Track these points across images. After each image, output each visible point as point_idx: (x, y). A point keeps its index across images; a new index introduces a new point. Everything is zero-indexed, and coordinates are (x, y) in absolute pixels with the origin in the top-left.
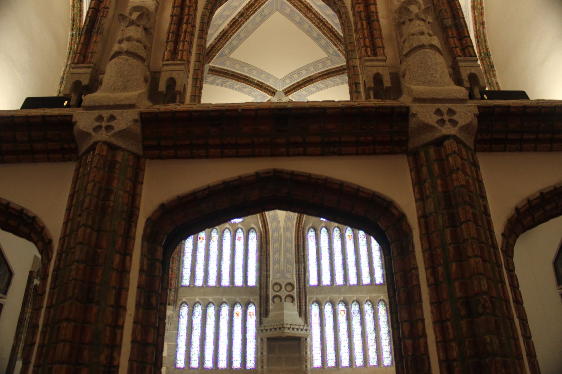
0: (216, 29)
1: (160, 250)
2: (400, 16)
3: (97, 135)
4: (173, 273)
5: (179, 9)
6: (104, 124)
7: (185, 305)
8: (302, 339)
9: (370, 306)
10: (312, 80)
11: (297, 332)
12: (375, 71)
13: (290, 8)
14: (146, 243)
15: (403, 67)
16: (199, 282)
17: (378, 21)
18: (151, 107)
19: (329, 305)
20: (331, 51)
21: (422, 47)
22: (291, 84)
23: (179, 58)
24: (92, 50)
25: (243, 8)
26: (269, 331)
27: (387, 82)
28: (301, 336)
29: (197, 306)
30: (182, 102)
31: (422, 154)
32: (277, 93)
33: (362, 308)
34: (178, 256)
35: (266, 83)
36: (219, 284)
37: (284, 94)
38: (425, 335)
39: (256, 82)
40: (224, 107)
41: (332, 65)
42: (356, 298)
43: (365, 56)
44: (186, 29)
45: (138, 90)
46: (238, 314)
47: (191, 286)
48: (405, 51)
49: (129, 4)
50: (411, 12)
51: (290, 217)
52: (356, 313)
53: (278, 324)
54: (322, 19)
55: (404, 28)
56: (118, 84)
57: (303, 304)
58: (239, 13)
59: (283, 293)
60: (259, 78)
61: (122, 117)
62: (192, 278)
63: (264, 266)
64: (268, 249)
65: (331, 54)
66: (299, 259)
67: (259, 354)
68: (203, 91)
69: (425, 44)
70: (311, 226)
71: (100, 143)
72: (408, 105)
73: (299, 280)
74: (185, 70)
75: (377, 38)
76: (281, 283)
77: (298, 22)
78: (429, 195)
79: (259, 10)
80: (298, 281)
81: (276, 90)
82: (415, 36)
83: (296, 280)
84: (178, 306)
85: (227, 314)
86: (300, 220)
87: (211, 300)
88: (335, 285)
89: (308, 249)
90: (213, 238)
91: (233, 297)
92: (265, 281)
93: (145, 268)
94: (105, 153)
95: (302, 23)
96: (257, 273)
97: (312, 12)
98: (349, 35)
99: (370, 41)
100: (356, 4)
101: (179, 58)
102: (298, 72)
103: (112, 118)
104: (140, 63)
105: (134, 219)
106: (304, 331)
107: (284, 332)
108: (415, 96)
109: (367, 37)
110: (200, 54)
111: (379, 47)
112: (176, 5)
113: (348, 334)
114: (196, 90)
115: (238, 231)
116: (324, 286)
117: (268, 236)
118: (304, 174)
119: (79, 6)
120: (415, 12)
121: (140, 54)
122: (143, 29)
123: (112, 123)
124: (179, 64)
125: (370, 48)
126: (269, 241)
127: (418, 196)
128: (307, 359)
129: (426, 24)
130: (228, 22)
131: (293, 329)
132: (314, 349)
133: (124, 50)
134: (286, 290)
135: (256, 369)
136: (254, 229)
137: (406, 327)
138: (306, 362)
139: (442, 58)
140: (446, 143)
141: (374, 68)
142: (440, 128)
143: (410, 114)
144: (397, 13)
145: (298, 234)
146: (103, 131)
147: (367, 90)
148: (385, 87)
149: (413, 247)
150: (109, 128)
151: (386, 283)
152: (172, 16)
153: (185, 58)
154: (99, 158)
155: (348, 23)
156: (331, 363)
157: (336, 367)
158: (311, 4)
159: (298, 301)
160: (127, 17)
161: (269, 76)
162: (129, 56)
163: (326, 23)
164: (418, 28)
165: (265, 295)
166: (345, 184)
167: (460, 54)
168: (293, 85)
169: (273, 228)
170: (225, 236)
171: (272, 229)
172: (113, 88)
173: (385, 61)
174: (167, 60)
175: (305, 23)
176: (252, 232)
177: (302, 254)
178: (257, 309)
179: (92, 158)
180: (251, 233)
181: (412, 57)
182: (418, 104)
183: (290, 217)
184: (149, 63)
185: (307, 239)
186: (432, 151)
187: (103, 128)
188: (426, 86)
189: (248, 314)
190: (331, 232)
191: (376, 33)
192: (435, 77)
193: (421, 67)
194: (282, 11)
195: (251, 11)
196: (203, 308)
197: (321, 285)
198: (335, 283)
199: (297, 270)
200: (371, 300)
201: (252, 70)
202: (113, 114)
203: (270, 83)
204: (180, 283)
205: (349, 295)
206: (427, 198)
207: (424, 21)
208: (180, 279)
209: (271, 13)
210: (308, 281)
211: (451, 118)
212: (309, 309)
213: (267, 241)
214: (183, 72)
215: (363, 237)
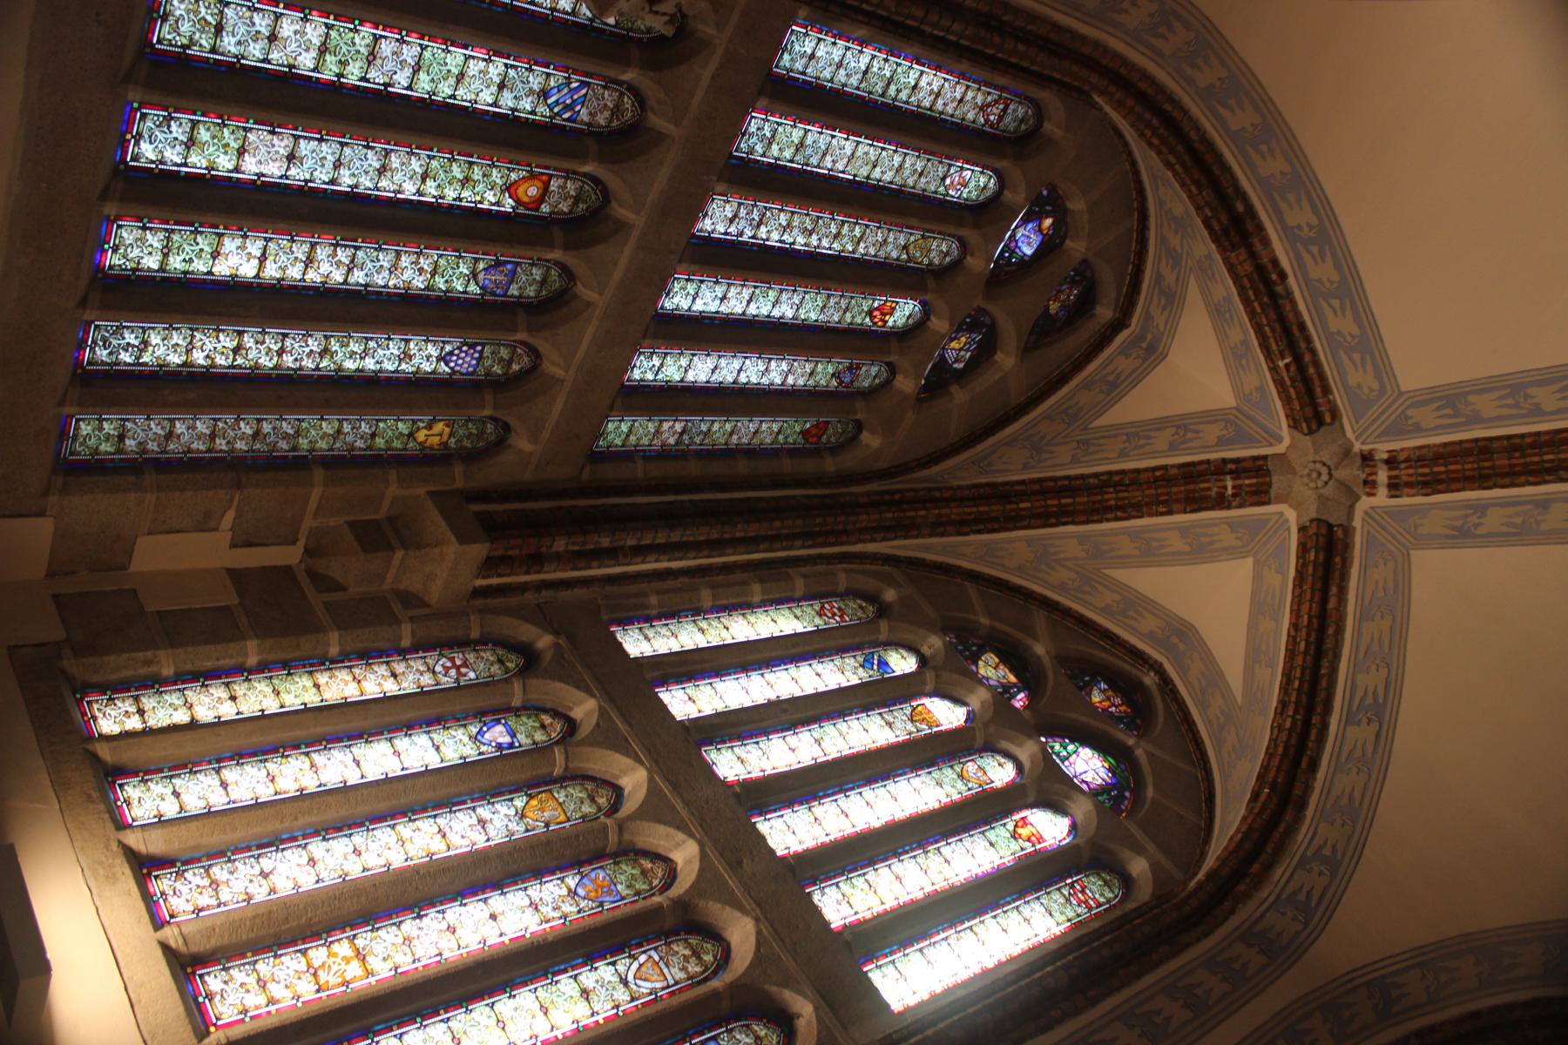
9: (497, 369)
19: (617, 110)
42: (589, 305)
70: (1047, 125)
205: (623, 262)
210: (814, 23)
215: (847, 380)
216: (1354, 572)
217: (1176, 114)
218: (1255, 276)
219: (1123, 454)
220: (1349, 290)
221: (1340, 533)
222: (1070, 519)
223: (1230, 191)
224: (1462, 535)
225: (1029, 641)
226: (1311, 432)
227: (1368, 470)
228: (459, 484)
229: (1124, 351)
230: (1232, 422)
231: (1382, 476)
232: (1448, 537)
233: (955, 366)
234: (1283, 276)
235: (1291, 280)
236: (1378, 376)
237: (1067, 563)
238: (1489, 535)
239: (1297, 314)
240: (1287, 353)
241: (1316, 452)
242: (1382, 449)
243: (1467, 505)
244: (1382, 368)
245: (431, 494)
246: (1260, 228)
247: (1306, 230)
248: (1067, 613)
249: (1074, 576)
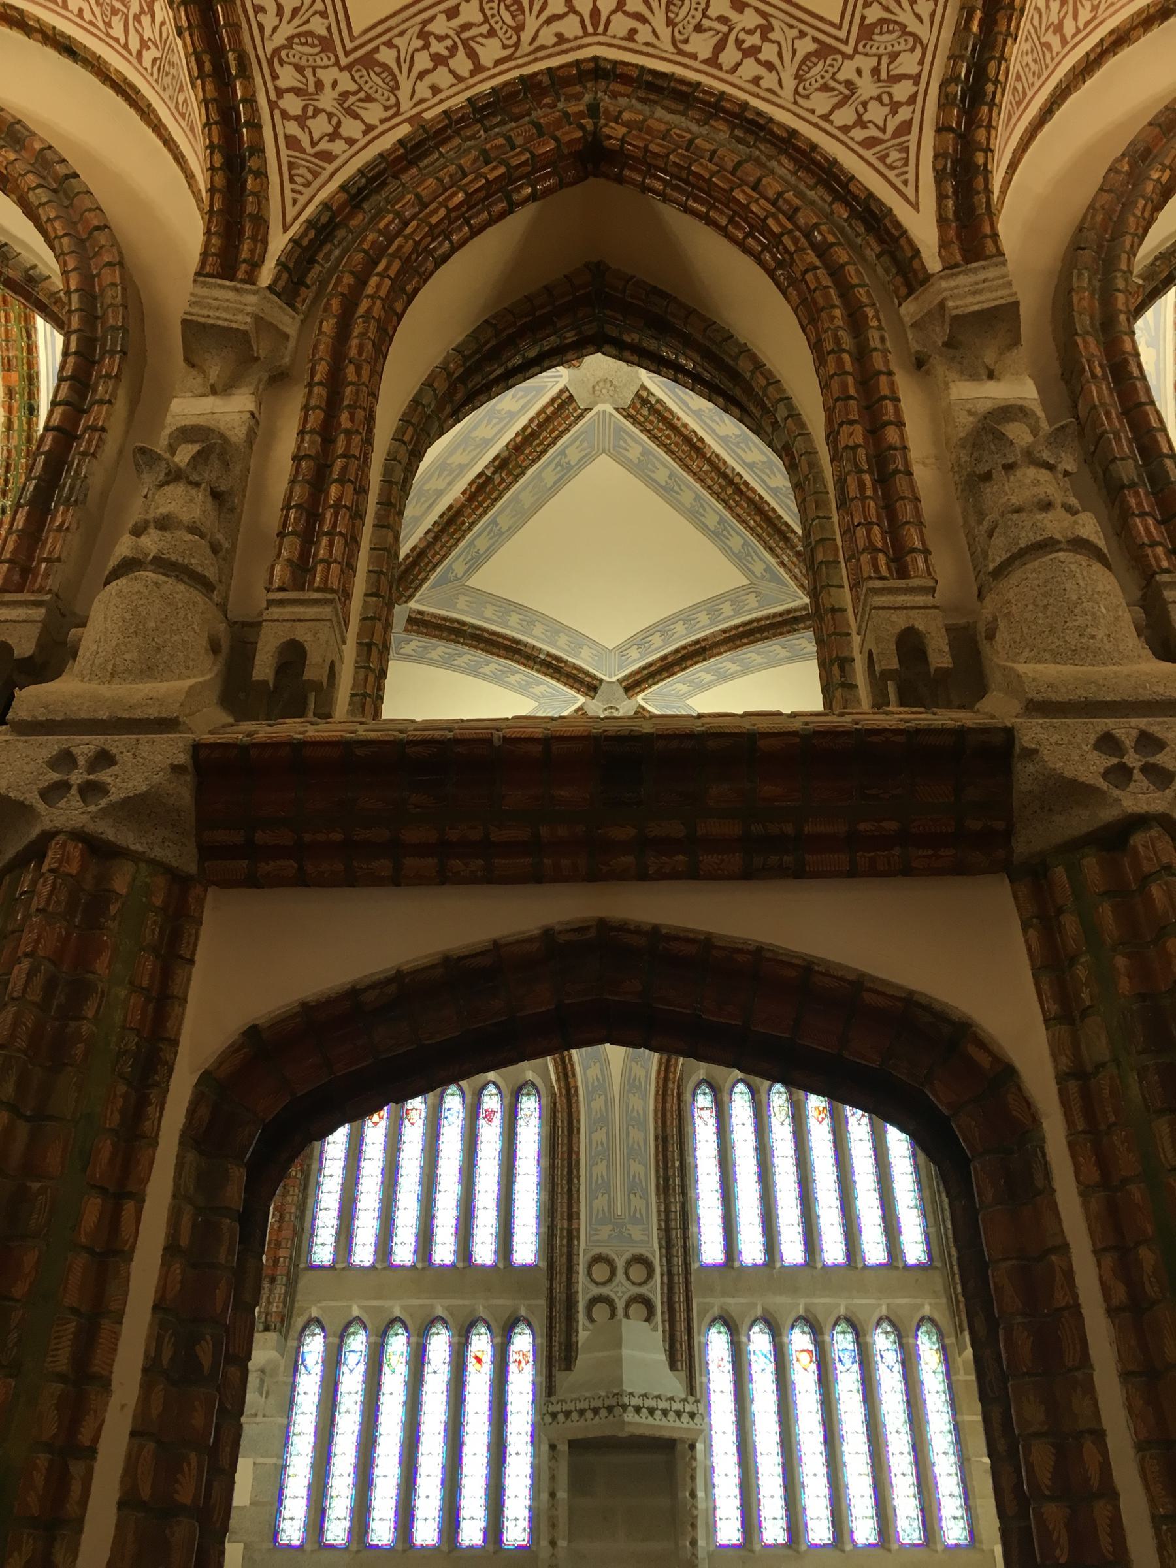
0: (427, 505)
1: (238, 1174)
2: (976, 454)
3: (53, 810)
4: (285, 1225)
5: (318, 439)
6: (76, 778)
7: (317, 1331)
8: (679, 1447)
9: (892, 1338)
10: (704, 650)
11: (664, 1422)
12: (900, 621)
13: (640, 444)
14: (191, 1156)
15: (988, 609)
16: (364, 1254)
17: (910, 474)
18: (229, 729)
19: (761, 1331)
20: (759, 568)
21: (1047, 546)
22: (643, 663)
23: (316, 585)
24: (51, 552)
25: (507, 446)
26: (575, 1416)
27: (940, 656)
28: (676, 1435)
29: (353, 1333)
30: (327, 716)
31: (1060, 873)
32: (603, 688)
33: (866, 1343)
34: (302, 1171)
35: (570, 659)
36: (423, 1261)
37: (622, 691)
38: (1110, 1493)
39: (542, 656)
40: (450, 730)
41: (761, 606)
42: (847, 1308)
43: (870, 578)
44: (340, 499)
45: (189, 677)
46: (479, 1360)
47: (339, 1266)
48: (994, 560)
49: (169, 419)
50: (1012, 443)
52: (847, 1361)
53: (603, 1394)
55: (989, 490)
56: (127, 656)
57: (681, 1327)
58: (494, 459)
59: (620, 1289)
60: (553, 644)
61: (135, 756)
62: (343, 1238)
63: (562, 1202)
64: (575, 1149)
66: (666, 1179)
67: (545, 1496)
68: (388, 683)
69: (1058, 536)
71: (61, 838)
72: (1009, 725)
73: (667, 1245)
74: (334, 619)
75: (907, 523)
76: (613, 1256)
77: (663, 484)
78: (1088, 1003)
79: (551, 452)
80: (664, 1251)
81: (601, 681)
82: (1024, 515)
83: (660, 1247)
84: (294, 1333)
85: (447, 1360)
87: (397, 1312)
88: (778, 1265)
89: (695, 1150)
90: (413, 1114)
91: (466, 1302)
92: (565, 1250)
93: (184, 1241)
94: (73, 869)
95: (676, 488)
96: (539, 1224)
97: (704, 456)
98: (818, 517)
99: (883, 532)
100: (841, 425)
101: (316, 585)
102: (663, 627)
103: (104, 759)
104: (197, 596)
105: (157, 1077)
106: (685, 1418)
107: (623, 1423)
108: (1030, 696)
109: (875, 520)
110: (381, 572)
111: (914, 550)
112: (308, 427)
113: (825, 1430)
114: (366, 680)
115: (485, 1092)
116: (744, 1268)
117: (574, 1106)
118: (691, 935)
119: (25, 427)
120: (1023, 443)
121: (199, 570)
122: (208, 493)
123: (104, 776)
124: (316, 602)
125: (886, 554)
126: (578, 1121)
127: (1054, 1008)
128: (696, 1517)
129: (1056, 478)
130: (462, 484)
131: (651, 1411)
132: (716, 1480)
133: (147, 555)
134: (628, 1278)
135: (534, 1548)
136: (533, 1084)
137: (1042, 1457)
138: (694, 1526)
139: (1112, 579)
140: (1138, 840)
141: (898, 612)
142: (1116, 793)
143: (1017, 750)
144: (964, 447)
145: (664, 1101)
146: (74, 799)
147: (878, 681)
148: (932, 670)
149: (1047, 1176)
150: (91, 790)
151: (939, 1264)
152: (296, 458)
153: (334, 583)
154: (54, 883)
155: (815, 482)
156: (774, 1531)
157: (790, 1547)
158: (701, 433)
159: (667, 1317)
160: (159, 457)
161: (580, 640)
162: (164, 574)
163: (742, 487)
164: (1035, 490)
165: (564, 1296)
166: (817, 968)
167: (1165, 564)
168: (650, 665)
169: (590, 1081)
170: (446, 1106)
171: (587, 1082)
172: (110, 668)
173: (933, 590)
174: (281, 589)
175: (683, 487)
176: (528, 1094)
177: (677, 1163)
178: (539, 1341)
179: (34, 883)
180: (525, 1099)
181: (1016, 576)
182: (1041, 721)
184: (226, 598)
185: (689, 1119)
186: (1091, 865)
187: (74, 791)
188: (1065, 664)
189: (513, 1357)
190: (764, 1097)
191: (906, 511)
192: (1093, 637)
193: (1046, 607)
194: (618, 452)
195: (530, 453)
196: (372, 1339)
197: (737, 1264)
198: (777, 1257)
199: (663, 1214)
200: (893, 1318)
202: (106, 747)
203: (583, 660)
204: (303, 1259)
206: (1085, 1013)
207: (1051, 467)
208: (305, 1243)
209: (586, 460)
210: (698, 1252)
211: (1152, 760)
212: (699, 1343)
213: (570, 1123)
214: (328, 623)
228: (953, 1340)
245: (960, 1354)
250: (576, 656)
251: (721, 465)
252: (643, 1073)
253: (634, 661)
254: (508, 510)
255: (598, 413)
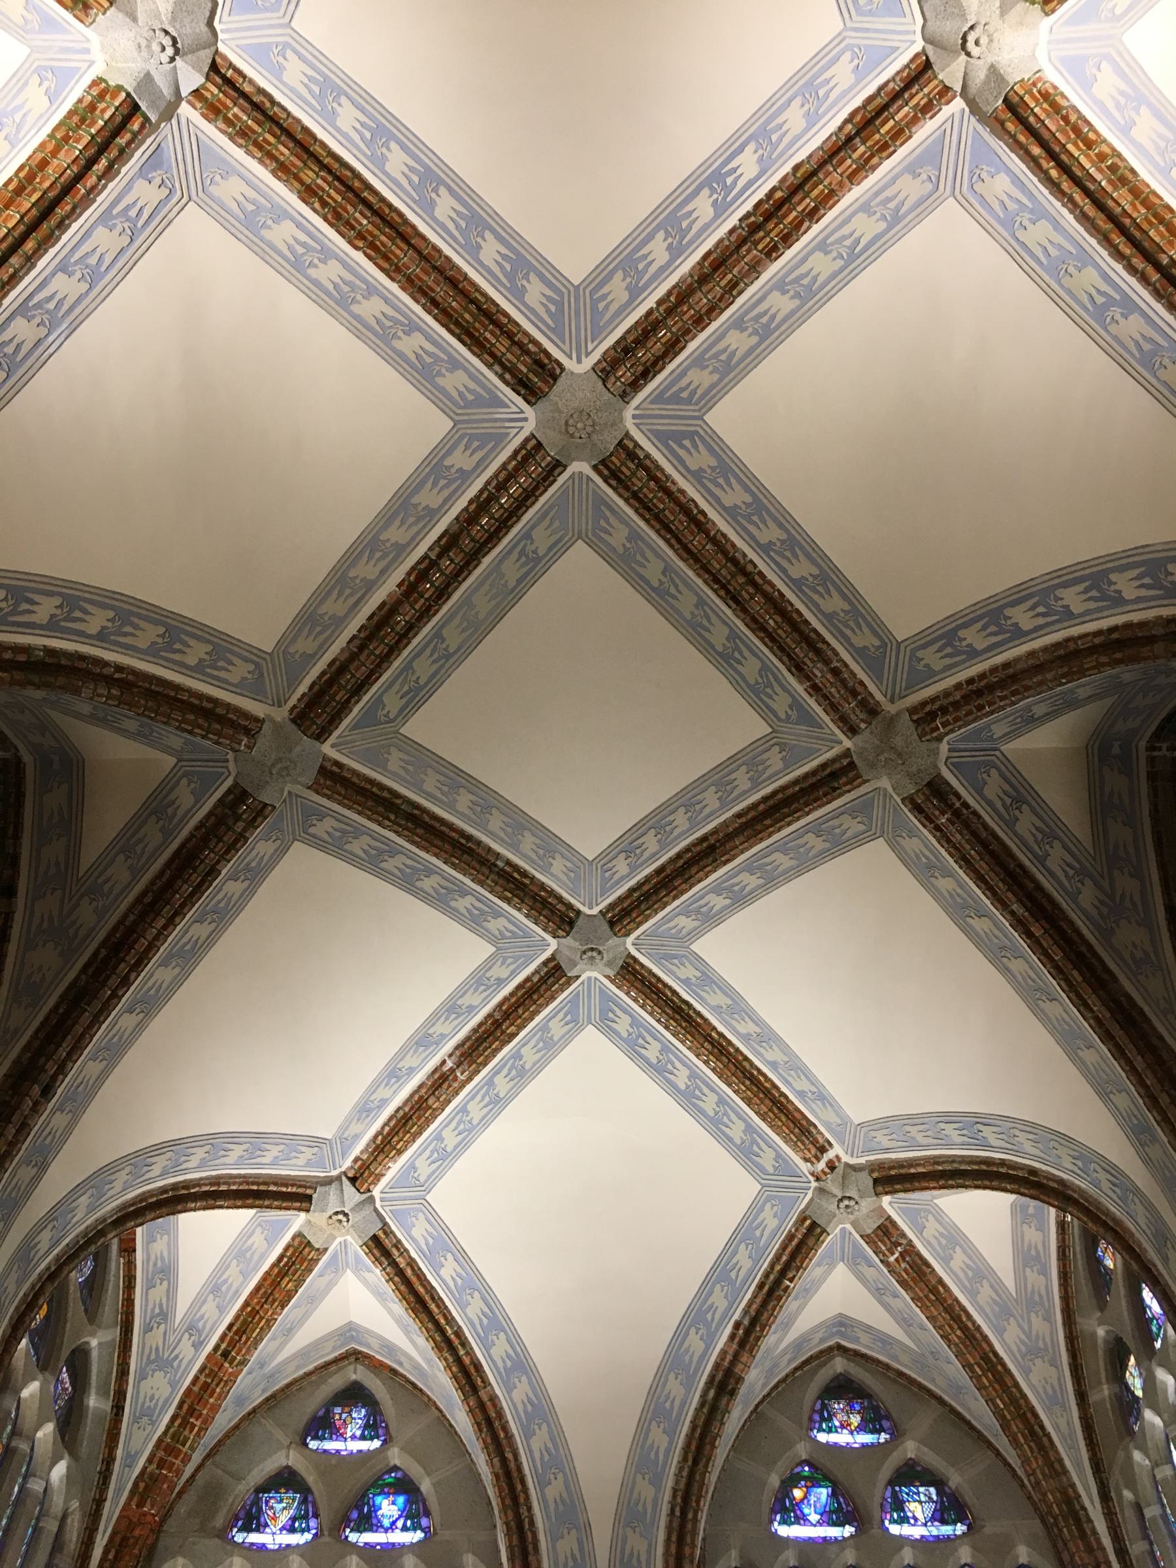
10: (712, 848)
13: (627, 525)
20: (781, 704)
22: (633, 882)
25: (457, 518)
32: (580, 922)
35: (538, 875)
37: (606, 927)
41: (788, 765)
51: (640, 1508)
54: (742, 562)
58: (440, 538)
60: (514, 846)
65: (783, 716)
77: (655, 584)
81: (578, 912)
86: (682, 1525)
95: (673, 590)
97: (707, 533)
102: (657, 821)
130: (399, 574)
158: (703, 505)
161: (551, 844)
163: (756, 577)
175: (681, 587)
183: (640, 1508)
201: (487, 809)
209: (558, 549)
216: (893, 1156)
217: (679, 1500)
218: (747, 1348)
219: (923, 1328)
220: (720, 1272)
221: (875, 1175)
222: (991, 1355)
223: (705, 1410)
224: (823, 1097)
225: (1100, 1341)
226: (824, 1231)
227: (824, 1178)
229: (857, 1340)
230: (855, 1262)
231: (822, 1165)
232: (831, 1105)
233: (935, 1497)
234: (737, 1325)
235: (736, 1317)
236: (762, 1210)
237: (1026, 1327)
238: (812, 1084)
239: (755, 1296)
240: (783, 1287)
241: (834, 1216)
242: (805, 1167)
243: (805, 1103)
244: (755, 1210)
246: (717, 1366)
247: (701, 1332)
248: (1066, 1299)
249: (1033, 1315)
250: (546, 869)
251: (728, 547)
252: (643, 1548)
253: (622, 879)
254: (456, 621)
255: (572, 477)
